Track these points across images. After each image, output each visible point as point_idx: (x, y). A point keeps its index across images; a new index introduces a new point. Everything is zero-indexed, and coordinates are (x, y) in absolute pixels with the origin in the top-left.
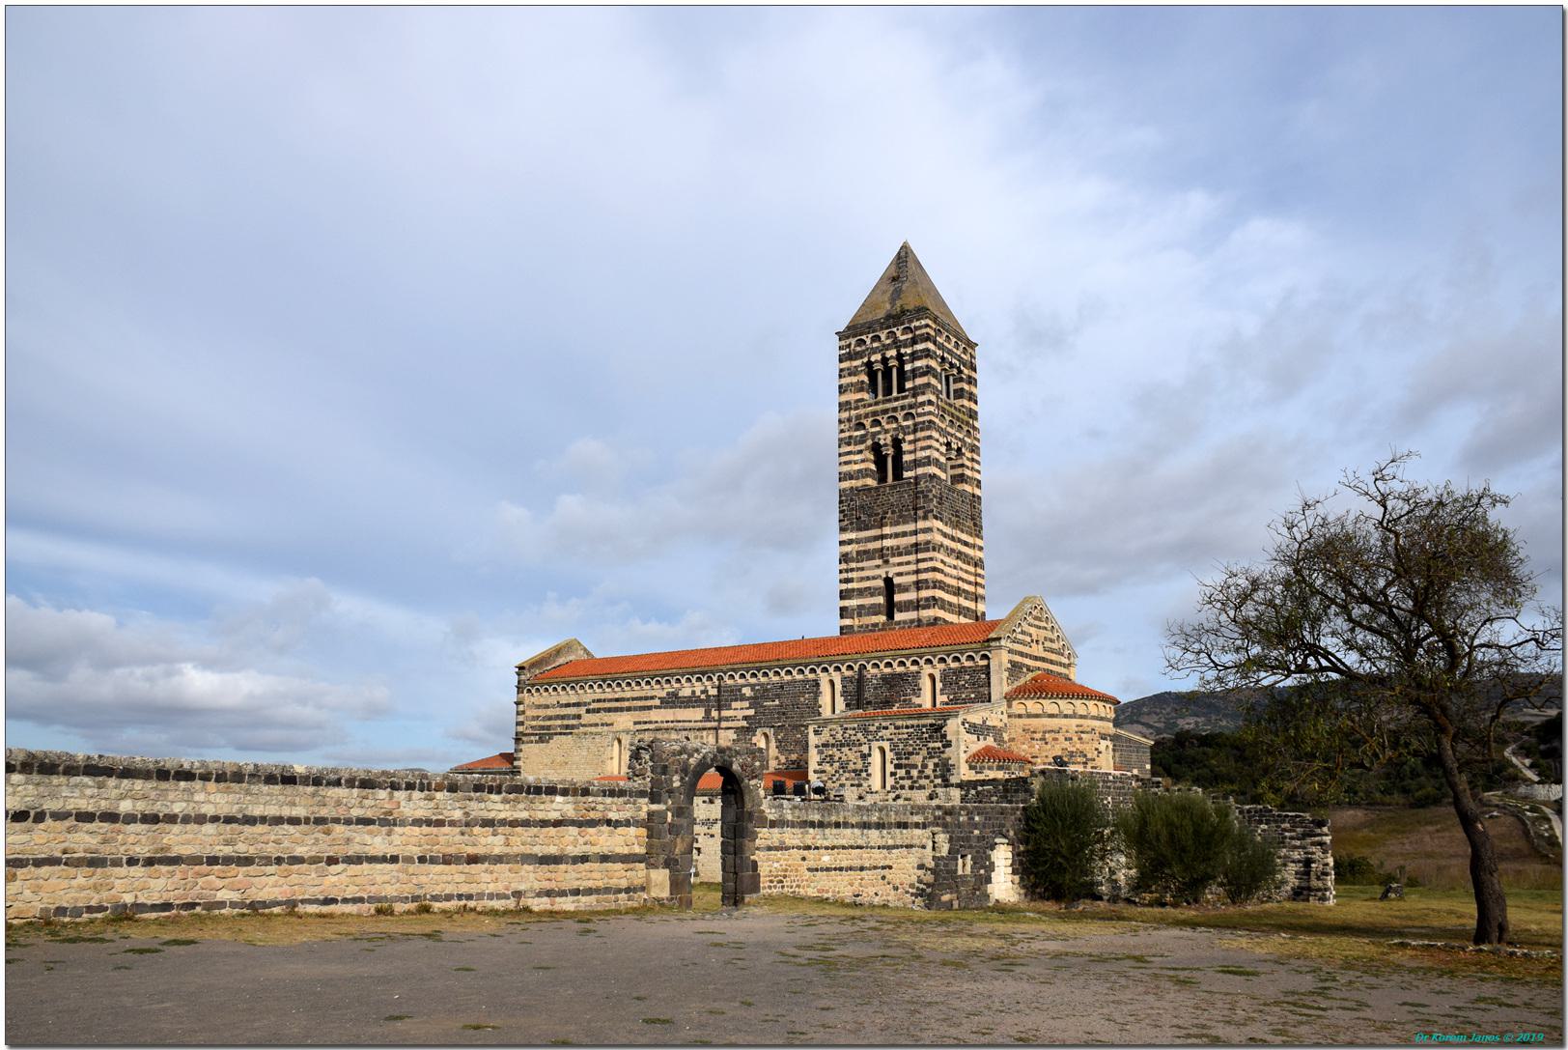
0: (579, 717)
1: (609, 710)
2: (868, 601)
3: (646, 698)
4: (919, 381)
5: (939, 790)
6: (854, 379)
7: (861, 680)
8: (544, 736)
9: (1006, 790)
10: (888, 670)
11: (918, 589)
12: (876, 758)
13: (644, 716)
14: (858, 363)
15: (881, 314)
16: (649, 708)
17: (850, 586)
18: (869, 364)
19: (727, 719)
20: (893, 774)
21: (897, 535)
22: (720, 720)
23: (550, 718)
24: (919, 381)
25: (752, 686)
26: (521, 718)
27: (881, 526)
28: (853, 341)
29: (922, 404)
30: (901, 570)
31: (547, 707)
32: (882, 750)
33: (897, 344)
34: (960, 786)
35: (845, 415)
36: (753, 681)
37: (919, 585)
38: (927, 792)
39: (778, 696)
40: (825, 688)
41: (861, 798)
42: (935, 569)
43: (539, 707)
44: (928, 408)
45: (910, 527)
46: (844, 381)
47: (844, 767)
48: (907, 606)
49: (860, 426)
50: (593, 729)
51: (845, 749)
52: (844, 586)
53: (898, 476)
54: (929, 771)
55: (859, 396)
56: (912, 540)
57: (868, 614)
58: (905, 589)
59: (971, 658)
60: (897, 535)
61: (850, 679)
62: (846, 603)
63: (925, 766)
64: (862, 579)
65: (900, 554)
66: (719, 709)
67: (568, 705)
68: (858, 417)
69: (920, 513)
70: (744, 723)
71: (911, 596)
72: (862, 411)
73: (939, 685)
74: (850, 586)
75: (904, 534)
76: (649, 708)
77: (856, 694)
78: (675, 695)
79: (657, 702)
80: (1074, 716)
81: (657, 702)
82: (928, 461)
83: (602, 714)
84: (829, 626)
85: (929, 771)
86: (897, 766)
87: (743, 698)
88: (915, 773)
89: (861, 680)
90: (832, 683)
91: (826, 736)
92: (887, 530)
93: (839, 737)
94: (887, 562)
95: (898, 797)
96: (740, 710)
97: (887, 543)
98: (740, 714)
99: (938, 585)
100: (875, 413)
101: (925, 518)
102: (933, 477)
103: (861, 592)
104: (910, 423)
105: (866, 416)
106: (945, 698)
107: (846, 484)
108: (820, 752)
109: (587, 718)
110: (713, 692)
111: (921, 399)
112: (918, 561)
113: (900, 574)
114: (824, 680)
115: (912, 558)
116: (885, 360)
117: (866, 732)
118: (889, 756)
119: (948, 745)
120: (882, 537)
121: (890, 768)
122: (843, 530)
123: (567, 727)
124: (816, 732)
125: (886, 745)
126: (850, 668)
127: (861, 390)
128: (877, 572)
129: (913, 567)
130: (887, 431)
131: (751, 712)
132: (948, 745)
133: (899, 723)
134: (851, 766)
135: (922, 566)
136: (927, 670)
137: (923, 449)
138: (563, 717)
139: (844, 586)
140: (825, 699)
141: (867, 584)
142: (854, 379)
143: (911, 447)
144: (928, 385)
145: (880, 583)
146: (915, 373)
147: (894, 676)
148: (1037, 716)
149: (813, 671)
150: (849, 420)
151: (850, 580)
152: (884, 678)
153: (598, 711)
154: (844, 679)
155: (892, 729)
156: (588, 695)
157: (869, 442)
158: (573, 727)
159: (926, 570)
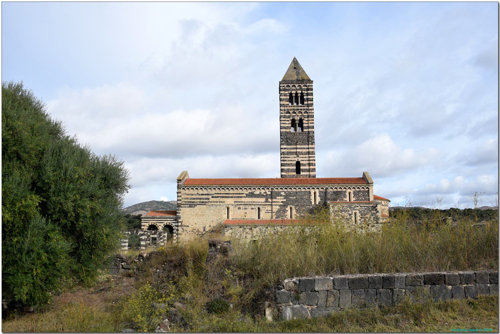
0: (208, 199)
1: (223, 197)
2: (291, 168)
3: (240, 194)
6: (286, 97)
10: (336, 190)
11: (309, 166)
12: (353, 216)
13: (239, 200)
14: (287, 92)
16: (241, 197)
17: (285, 162)
18: (291, 94)
19: (275, 202)
21: (301, 148)
23: (194, 199)
25: (285, 192)
26: (180, 198)
27: (296, 145)
28: (286, 85)
30: (303, 160)
31: (193, 195)
33: (301, 89)
36: (286, 190)
39: (295, 196)
40: (313, 194)
43: (188, 195)
45: (307, 146)
48: (305, 170)
49: (288, 112)
50: (215, 203)
51: (343, 212)
52: (283, 162)
56: (307, 150)
57: (291, 172)
58: (305, 165)
59: (363, 188)
60: (301, 148)
61: (322, 192)
62: (283, 167)
64: (289, 161)
65: (303, 154)
66: (272, 198)
68: (288, 110)
69: (310, 143)
71: (307, 167)
72: (289, 108)
73: (352, 195)
74: (285, 162)
75: (304, 148)
76: (241, 197)
79: (245, 195)
81: (245, 195)
84: (277, 175)
85: (372, 219)
88: (367, 219)
89: (326, 193)
90: (315, 193)
92: (298, 146)
94: (298, 156)
96: (280, 200)
97: (298, 150)
98: (280, 201)
103: (288, 165)
104: (306, 114)
105: (291, 110)
106: (354, 199)
109: (212, 200)
110: (270, 193)
112: (309, 157)
113: (303, 160)
114: (312, 191)
115: (307, 156)
116: (296, 94)
117: (350, 208)
118: (358, 214)
119: (378, 212)
120: (296, 148)
123: (203, 202)
125: (358, 212)
126: (322, 188)
128: (294, 159)
131: (285, 200)
132: (378, 212)
135: (311, 159)
136: (349, 190)
138: (200, 199)
139: (283, 162)
140: (312, 197)
141: (291, 162)
142: (286, 97)
143: (307, 122)
145: (295, 162)
147: (337, 192)
149: (309, 188)
150: (285, 110)
151: (286, 161)
152: (334, 192)
153: (215, 197)
154: (320, 192)
155: (359, 207)
156: (213, 192)
157: (291, 118)
158: (205, 202)
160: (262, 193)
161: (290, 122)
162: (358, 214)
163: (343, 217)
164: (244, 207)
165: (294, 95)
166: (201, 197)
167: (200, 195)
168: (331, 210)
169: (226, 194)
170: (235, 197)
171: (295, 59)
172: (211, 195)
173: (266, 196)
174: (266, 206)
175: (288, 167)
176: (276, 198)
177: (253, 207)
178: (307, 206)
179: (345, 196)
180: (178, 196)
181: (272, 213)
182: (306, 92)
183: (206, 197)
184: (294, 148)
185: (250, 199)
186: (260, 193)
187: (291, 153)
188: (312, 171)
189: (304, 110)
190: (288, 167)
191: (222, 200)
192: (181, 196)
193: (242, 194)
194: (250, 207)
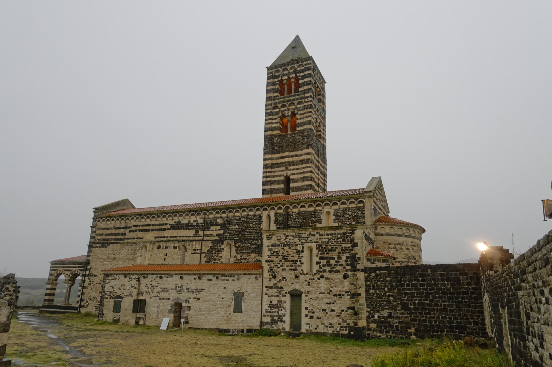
0: (125, 234)
3: (163, 225)
4: (306, 87)
5: (349, 273)
7: (287, 215)
8: (105, 244)
9: (397, 274)
11: (303, 181)
13: (162, 234)
14: (276, 80)
15: (288, 60)
16: (164, 230)
17: (268, 179)
18: (281, 81)
19: (207, 236)
20: (318, 263)
21: (292, 156)
22: (204, 235)
23: (109, 235)
24: (306, 87)
28: (274, 70)
29: (308, 97)
31: (108, 229)
32: (311, 250)
33: (295, 72)
34: (365, 270)
35: (270, 102)
37: (303, 179)
38: (341, 276)
40: (264, 218)
41: (297, 277)
42: (311, 172)
44: (310, 99)
46: (269, 88)
47: (285, 258)
51: (286, 248)
52: (265, 179)
53: (294, 128)
54: (342, 261)
55: (276, 94)
58: (295, 181)
60: (292, 156)
61: (280, 214)
63: (339, 258)
64: (274, 176)
65: (294, 165)
67: (119, 228)
70: (217, 238)
72: (277, 101)
75: (296, 156)
76: (164, 230)
77: (285, 223)
78: (179, 222)
79: (169, 227)
80: (410, 236)
81: (169, 227)
82: (310, 122)
83: (138, 233)
85: (342, 261)
86: (321, 258)
87: (217, 224)
88: (333, 262)
89: (287, 215)
90: (269, 216)
91: (274, 240)
92: (287, 154)
93: (283, 240)
95: (322, 277)
97: (287, 160)
98: (215, 233)
99: (312, 179)
100: (283, 102)
101: (307, 148)
102: (311, 129)
103: (272, 183)
105: (279, 103)
107: (269, 133)
108: (270, 250)
111: (307, 95)
112: (304, 168)
113: (294, 174)
114: (265, 214)
116: (289, 79)
117: (300, 237)
118: (315, 252)
119: (356, 245)
121: (316, 259)
122: (265, 153)
123: (118, 239)
124: (268, 238)
125: (314, 246)
126: (280, 208)
127: (276, 92)
129: (301, 171)
130: (288, 110)
131: (222, 232)
132: (356, 245)
133: (322, 232)
134: (290, 258)
136: (327, 209)
137: (307, 117)
138: (116, 234)
140: (264, 226)
142: (275, 87)
143: (302, 116)
144: (310, 89)
145: (282, 178)
146: (304, 84)
148: (391, 235)
150: (271, 105)
153: (136, 231)
154: (276, 214)
155: (317, 236)
157: (280, 115)
158: (121, 239)
159: (308, 172)
160: (192, 222)
161: (278, 120)
162: (315, 252)
163: (285, 258)
164: (165, 245)
165: (285, 82)
166: (117, 231)
167: (116, 228)
168: (266, 242)
169: (147, 225)
170: (156, 230)
171: (297, 37)
172: (129, 228)
173: (196, 227)
174: (194, 243)
175: (273, 187)
176: (209, 229)
177: (177, 245)
178: (253, 240)
179: (320, 221)
180: (92, 232)
181: (201, 253)
182: (301, 74)
183: (122, 231)
184: (282, 157)
185: (175, 233)
186: (189, 221)
187: (278, 165)
188: (306, 189)
189: (297, 99)
190: (273, 187)
191: (140, 234)
192: (95, 232)
193: (166, 224)
194: (172, 245)
